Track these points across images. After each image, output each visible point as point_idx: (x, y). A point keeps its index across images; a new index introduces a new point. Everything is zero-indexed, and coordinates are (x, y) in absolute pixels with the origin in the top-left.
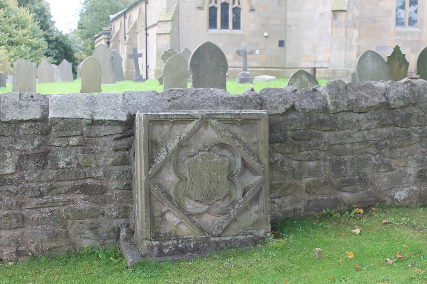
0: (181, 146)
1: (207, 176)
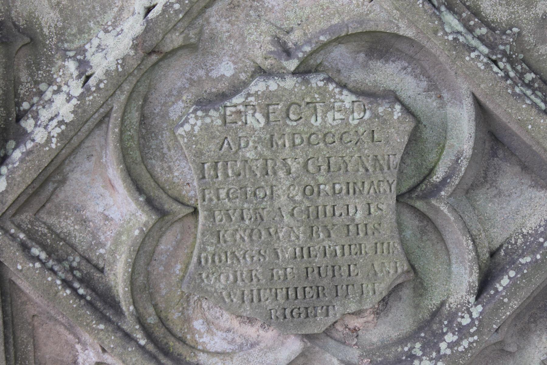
0: (153, 52)
1: (291, 199)
